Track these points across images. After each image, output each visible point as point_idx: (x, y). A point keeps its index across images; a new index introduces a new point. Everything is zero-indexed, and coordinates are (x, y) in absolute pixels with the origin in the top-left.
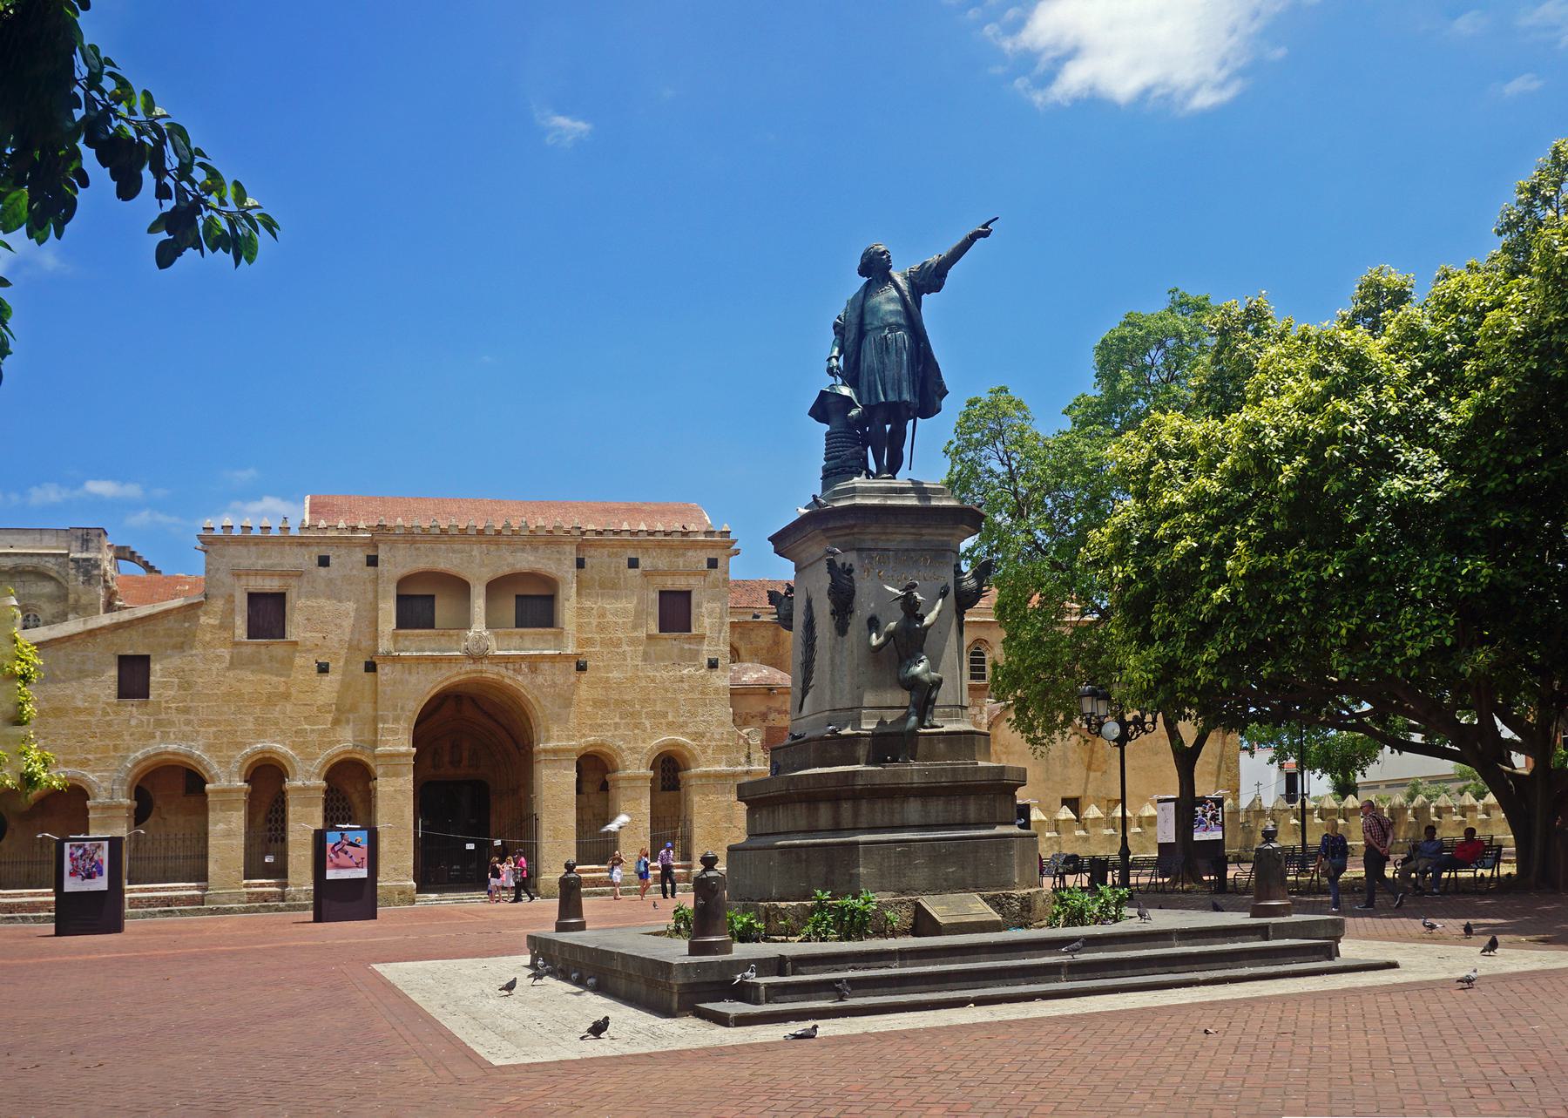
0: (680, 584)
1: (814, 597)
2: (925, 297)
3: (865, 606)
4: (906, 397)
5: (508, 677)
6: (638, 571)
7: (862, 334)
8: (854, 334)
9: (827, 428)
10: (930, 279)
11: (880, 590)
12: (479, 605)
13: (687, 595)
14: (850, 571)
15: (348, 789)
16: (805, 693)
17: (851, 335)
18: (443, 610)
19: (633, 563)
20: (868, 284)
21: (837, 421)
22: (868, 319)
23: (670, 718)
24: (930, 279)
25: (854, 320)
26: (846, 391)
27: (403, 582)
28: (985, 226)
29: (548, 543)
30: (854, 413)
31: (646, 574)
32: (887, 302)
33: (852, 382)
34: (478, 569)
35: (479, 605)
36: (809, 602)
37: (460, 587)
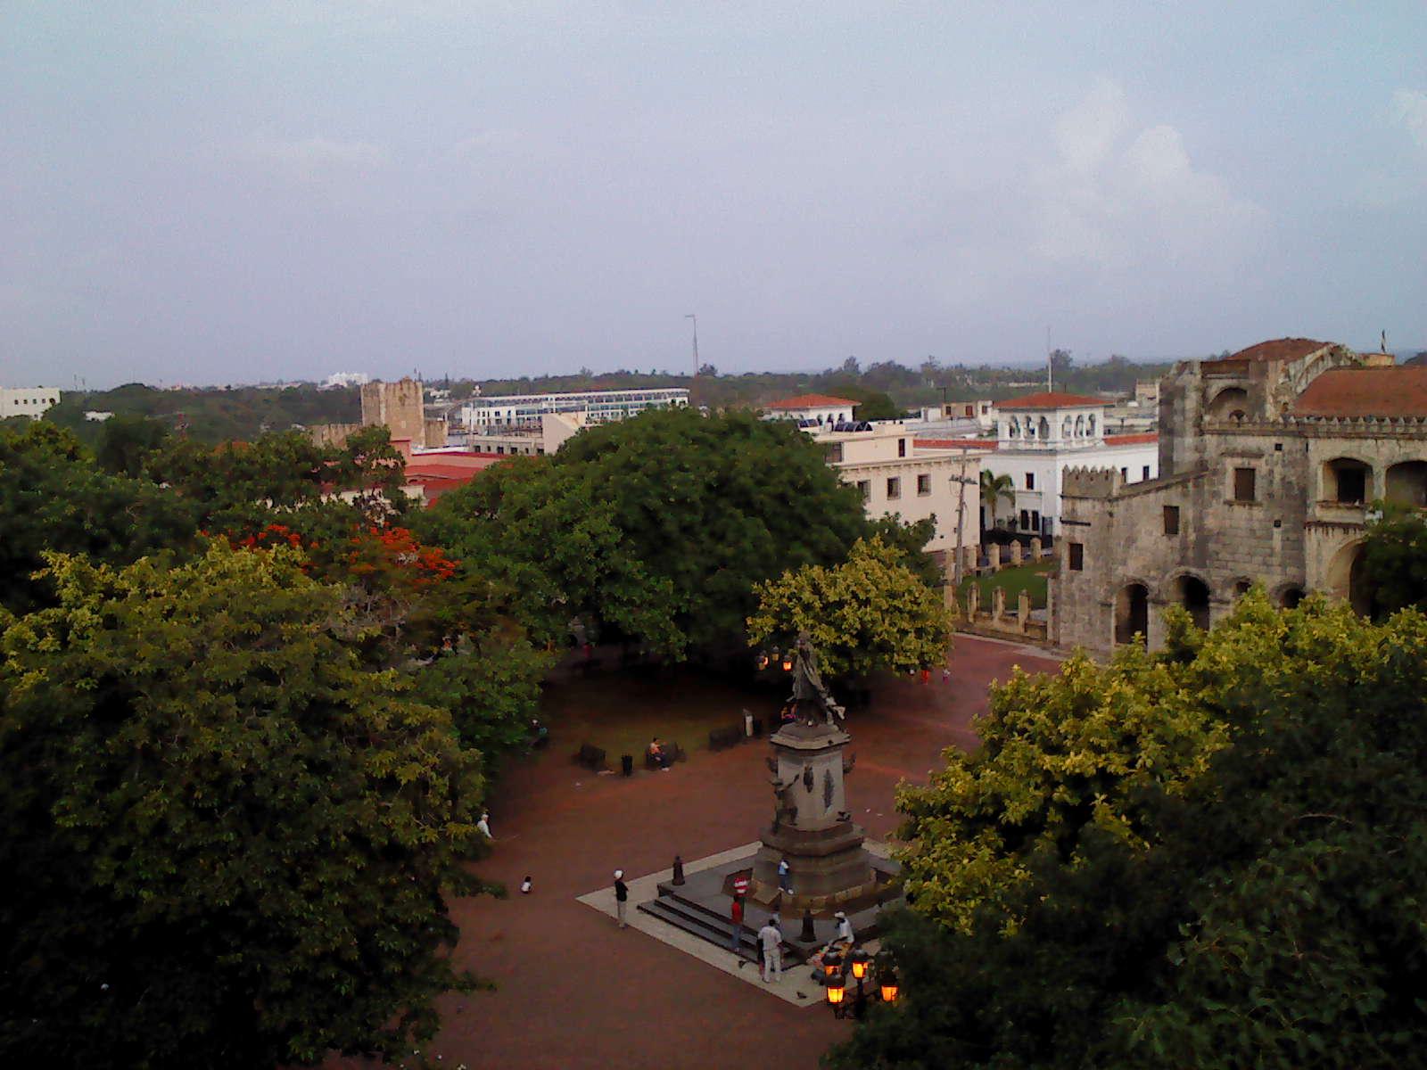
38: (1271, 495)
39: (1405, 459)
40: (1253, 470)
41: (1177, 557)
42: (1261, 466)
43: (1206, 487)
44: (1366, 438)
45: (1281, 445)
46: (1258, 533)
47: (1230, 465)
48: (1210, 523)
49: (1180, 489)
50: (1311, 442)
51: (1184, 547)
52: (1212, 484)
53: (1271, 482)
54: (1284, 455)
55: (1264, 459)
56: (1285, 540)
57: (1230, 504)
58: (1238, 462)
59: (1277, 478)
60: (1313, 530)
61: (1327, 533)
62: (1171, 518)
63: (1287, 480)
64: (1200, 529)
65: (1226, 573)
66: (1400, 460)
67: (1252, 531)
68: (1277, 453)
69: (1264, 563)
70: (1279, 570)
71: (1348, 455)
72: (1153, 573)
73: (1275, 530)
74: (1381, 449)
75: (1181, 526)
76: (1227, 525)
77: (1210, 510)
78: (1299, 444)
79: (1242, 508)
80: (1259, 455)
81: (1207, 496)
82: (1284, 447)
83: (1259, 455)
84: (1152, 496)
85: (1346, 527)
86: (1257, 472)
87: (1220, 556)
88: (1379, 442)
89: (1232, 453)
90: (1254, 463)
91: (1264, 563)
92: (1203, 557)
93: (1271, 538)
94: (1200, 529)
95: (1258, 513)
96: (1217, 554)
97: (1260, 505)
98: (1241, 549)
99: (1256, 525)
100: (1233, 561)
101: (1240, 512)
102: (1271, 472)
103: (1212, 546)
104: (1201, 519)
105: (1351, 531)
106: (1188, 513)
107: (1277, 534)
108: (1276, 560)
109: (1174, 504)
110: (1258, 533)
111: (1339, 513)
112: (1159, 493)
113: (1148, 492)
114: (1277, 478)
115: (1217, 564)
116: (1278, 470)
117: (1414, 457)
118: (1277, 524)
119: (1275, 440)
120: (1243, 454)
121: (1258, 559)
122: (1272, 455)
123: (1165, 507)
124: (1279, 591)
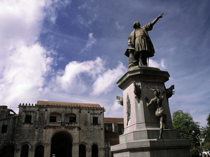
2: (148, 31)
7: (135, 38)
10: (150, 28)
13: (97, 118)
19: (89, 112)
22: (136, 35)
24: (150, 28)
25: (133, 35)
29: (75, 109)
31: (91, 114)
53: (36, 118)
55: (34, 113)
56: (39, 132)
65: (21, 142)
70: (36, 140)
83: (33, 112)
92: (13, 137)
95: (32, 126)
96: (18, 137)
100: (23, 138)
102: (36, 116)
108: (36, 137)
110: (31, 131)
114: (38, 117)
118: (37, 128)
122: (36, 112)
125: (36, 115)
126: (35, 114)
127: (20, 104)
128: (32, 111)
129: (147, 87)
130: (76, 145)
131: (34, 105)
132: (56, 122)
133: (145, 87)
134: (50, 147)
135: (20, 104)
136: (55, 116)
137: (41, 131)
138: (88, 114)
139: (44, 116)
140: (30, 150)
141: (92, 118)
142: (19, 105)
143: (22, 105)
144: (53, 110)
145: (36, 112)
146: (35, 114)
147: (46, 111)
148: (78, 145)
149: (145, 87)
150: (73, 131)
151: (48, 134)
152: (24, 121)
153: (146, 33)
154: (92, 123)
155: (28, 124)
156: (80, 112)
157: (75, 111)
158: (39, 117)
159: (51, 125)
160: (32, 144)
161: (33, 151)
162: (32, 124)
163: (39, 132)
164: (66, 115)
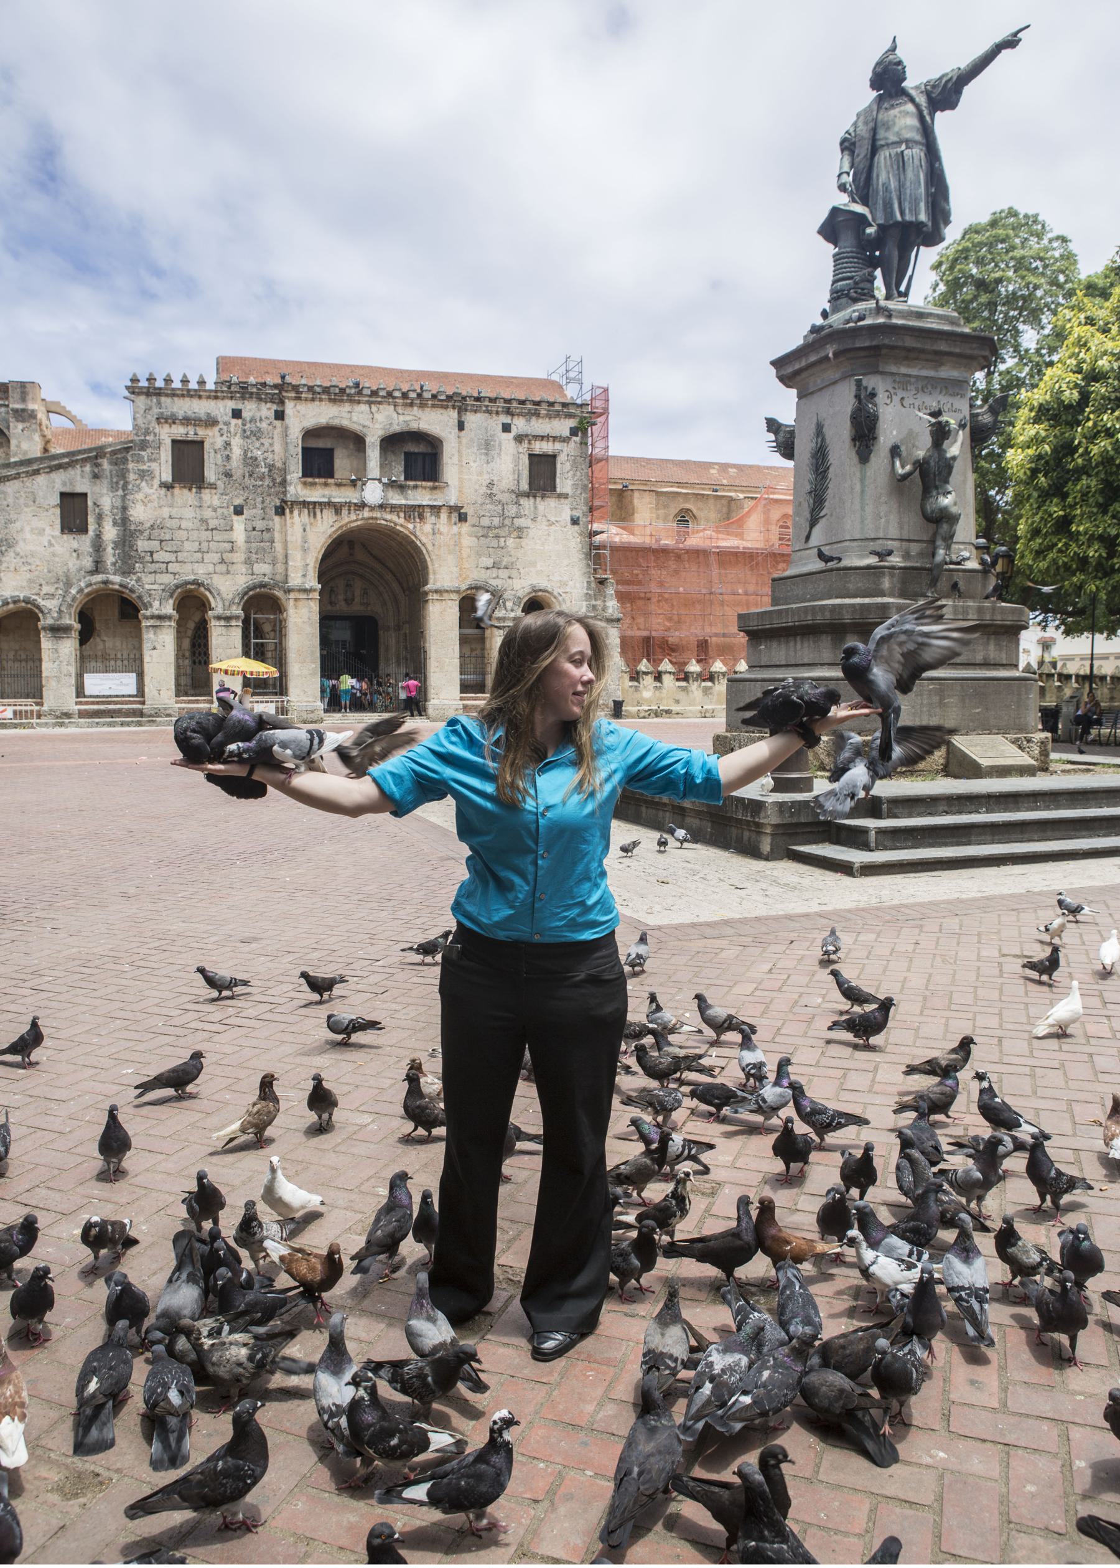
0: (546, 447)
1: (826, 424)
3: (888, 433)
4: (923, 217)
5: (398, 521)
6: (511, 435)
7: (874, 150)
8: (862, 149)
9: (830, 249)
10: (946, 94)
11: (903, 420)
12: (373, 455)
14: (873, 395)
15: (261, 615)
16: (813, 522)
17: (863, 151)
18: (342, 463)
19: (506, 428)
20: (880, 97)
21: (848, 241)
22: (881, 134)
23: (539, 568)
24: (946, 94)
26: (859, 208)
27: (310, 434)
28: (1015, 34)
29: (433, 406)
30: (870, 230)
31: (519, 439)
32: (903, 120)
33: (865, 202)
34: (375, 422)
35: (373, 455)
36: (819, 431)
37: (358, 441)
38: (228, 475)
39: (405, 429)
40: (202, 443)
41: (88, 563)
42: (213, 439)
43: (131, 466)
44: (359, 402)
45: (240, 411)
46: (213, 523)
47: (167, 434)
48: (139, 513)
49: (88, 468)
50: (290, 407)
51: (98, 546)
52: (139, 460)
53: (228, 458)
54: (244, 425)
55: (216, 429)
57: (168, 487)
58: (179, 431)
59: (237, 452)
60: (296, 512)
61: (315, 514)
62: (74, 512)
63: (249, 455)
64: (124, 522)
65: (167, 579)
66: (396, 428)
67: (204, 521)
68: (234, 421)
69: (223, 561)
70: (243, 569)
71: (336, 422)
72: (46, 589)
73: (235, 518)
74: (376, 416)
75: (91, 519)
76: (166, 516)
77: (140, 496)
78: (267, 410)
79: (186, 491)
80: (211, 422)
81: (132, 477)
82: (244, 414)
83: (211, 422)
84: (41, 479)
85: (337, 508)
86: (206, 445)
87: (155, 555)
88: (374, 408)
89: (172, 420)
90: (202, 432)
91: (223, 561)
92: (128, 558)
93: (231, 529)
94: (124, 522)
96: (152, 553)
97: (212, 486)
98: (187, 546)
99: (208, 513)
101: (184, 496)
102: (227, 444)
103: (142, 545)
104: (125, 509)
105: (345, 512)
106: (103, 498)
107: (239, 524)
108: (239, 557)
109: (79, 489)
111: (327, 491)
112: (53, 475)
113: (37, 472)
114: (237, 452)
115: (153, 567)
116: (237, 443)
117: (414, 426)
118: (239, 511)
119: (231, 405)
120: (187, 421)
121: (216, 557)
122: (227, 424)
123: (62, 495)
124: (246, 593)
125: (224, 438)
126: (222, 435)
127: (135, 380)
128: (203, 417)
129: (902, 399)
130: (446, 596)
131: (210, 386)
132: (332, 476)
133: (896, 399)
134: (315, 607)
135: (135, 380)
136: (329, 446)
137: (260, 525)
138: (505, 435)
139: (271, 445)
140: (219, 618)
141: (525, 460)
142: (129, 384)
143: (144, 383)
144: (322, 414)
145: (227, 424)
146: (222, 435)
147: (280, 415)
148: (455, 596)
149: (896, 399)
150: (428, 528)
151: (303, 543)
152: (167, 477)
153: (928, 118)
154: (525, 486)
155: (190, 490)
156: (461, 426)
157: (435, 422)
158: (246, 452)
159: (316, 495)
160: (223, 589)
161: (234, 623)
162: (212, 486)
163: (254, 529)
164: (391, 442)
